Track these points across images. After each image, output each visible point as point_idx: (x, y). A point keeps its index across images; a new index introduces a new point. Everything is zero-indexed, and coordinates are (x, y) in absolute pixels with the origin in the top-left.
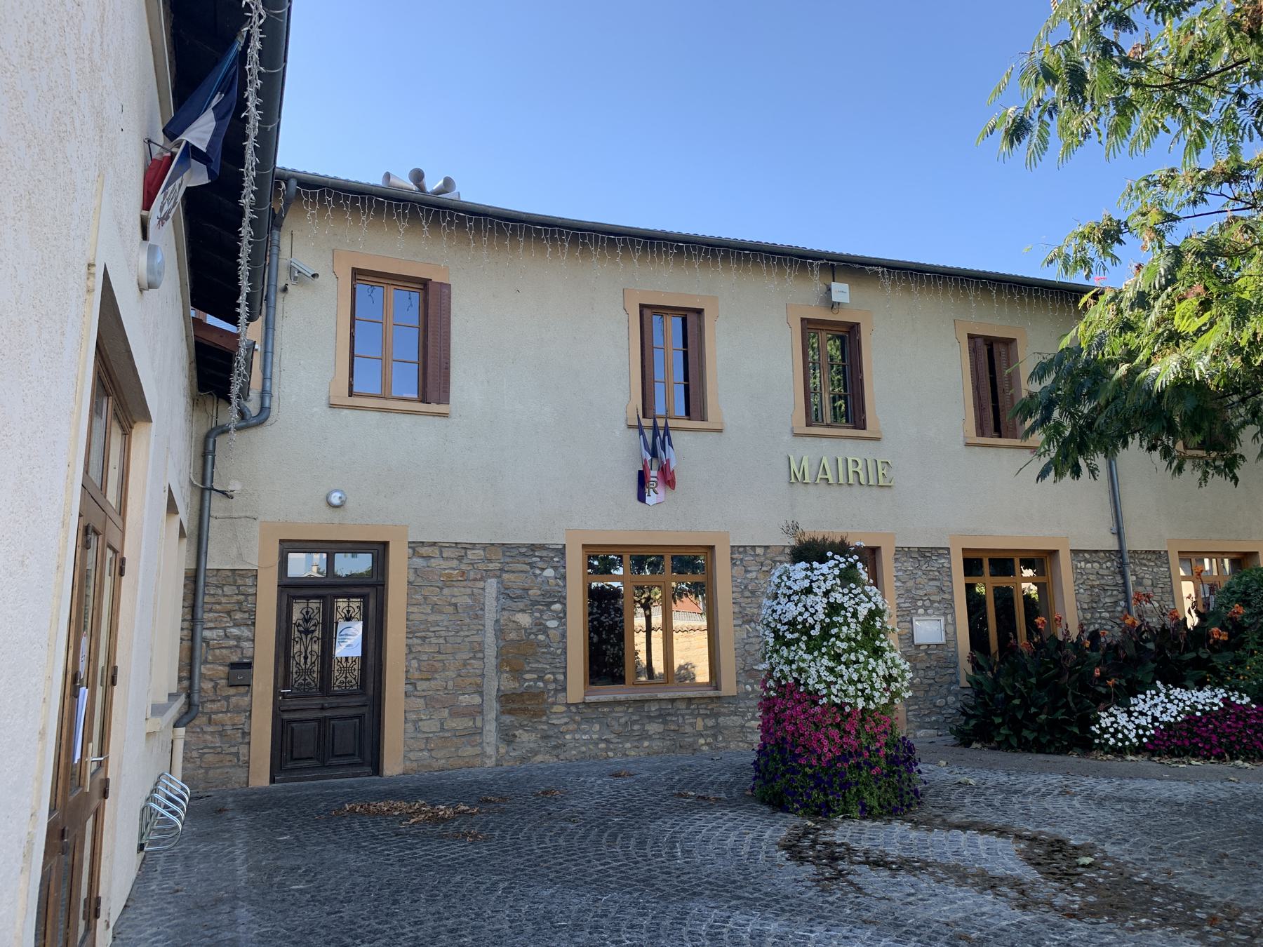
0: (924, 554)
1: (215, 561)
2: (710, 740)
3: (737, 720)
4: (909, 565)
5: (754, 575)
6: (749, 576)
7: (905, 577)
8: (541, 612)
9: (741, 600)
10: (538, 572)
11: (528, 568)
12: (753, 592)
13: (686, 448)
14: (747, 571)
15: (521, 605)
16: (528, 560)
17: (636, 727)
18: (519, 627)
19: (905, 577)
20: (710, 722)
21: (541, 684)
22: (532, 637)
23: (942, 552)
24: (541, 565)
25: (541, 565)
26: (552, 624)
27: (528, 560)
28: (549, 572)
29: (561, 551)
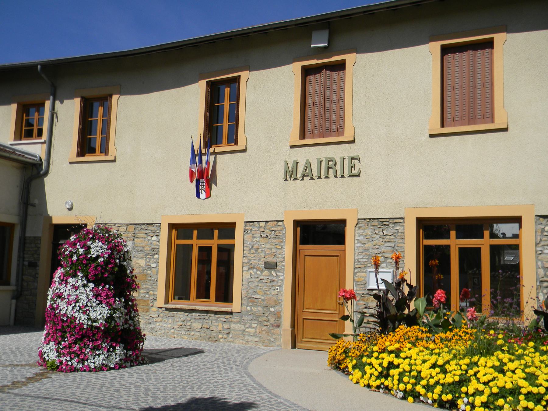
0: (384, 222)
1: (28, 234)
2: (225, 336)
3: (240, 327)
4: (369, 231)
5: (257, 239)
6: (254, 240)
7: (365, 240)
8: (150, 259)
9: (249, 255)
10: (149, 238)
11: (145, 236)
12: (257, 250)
13: (226, 165)
14: (254, 237)
15: (141, 255)
16: (146, 232)
17: (189, 324)
18: (140, 267)
19: (365, 240)
20: (226, 326)
21: (147, 296)
22: (145, 271)
23: (397, 221)
24: (151, 234)
25: (151, 234)
26: (154, 265)
27: (146, 232)
28: (154, 238)
29: (159, 226)
